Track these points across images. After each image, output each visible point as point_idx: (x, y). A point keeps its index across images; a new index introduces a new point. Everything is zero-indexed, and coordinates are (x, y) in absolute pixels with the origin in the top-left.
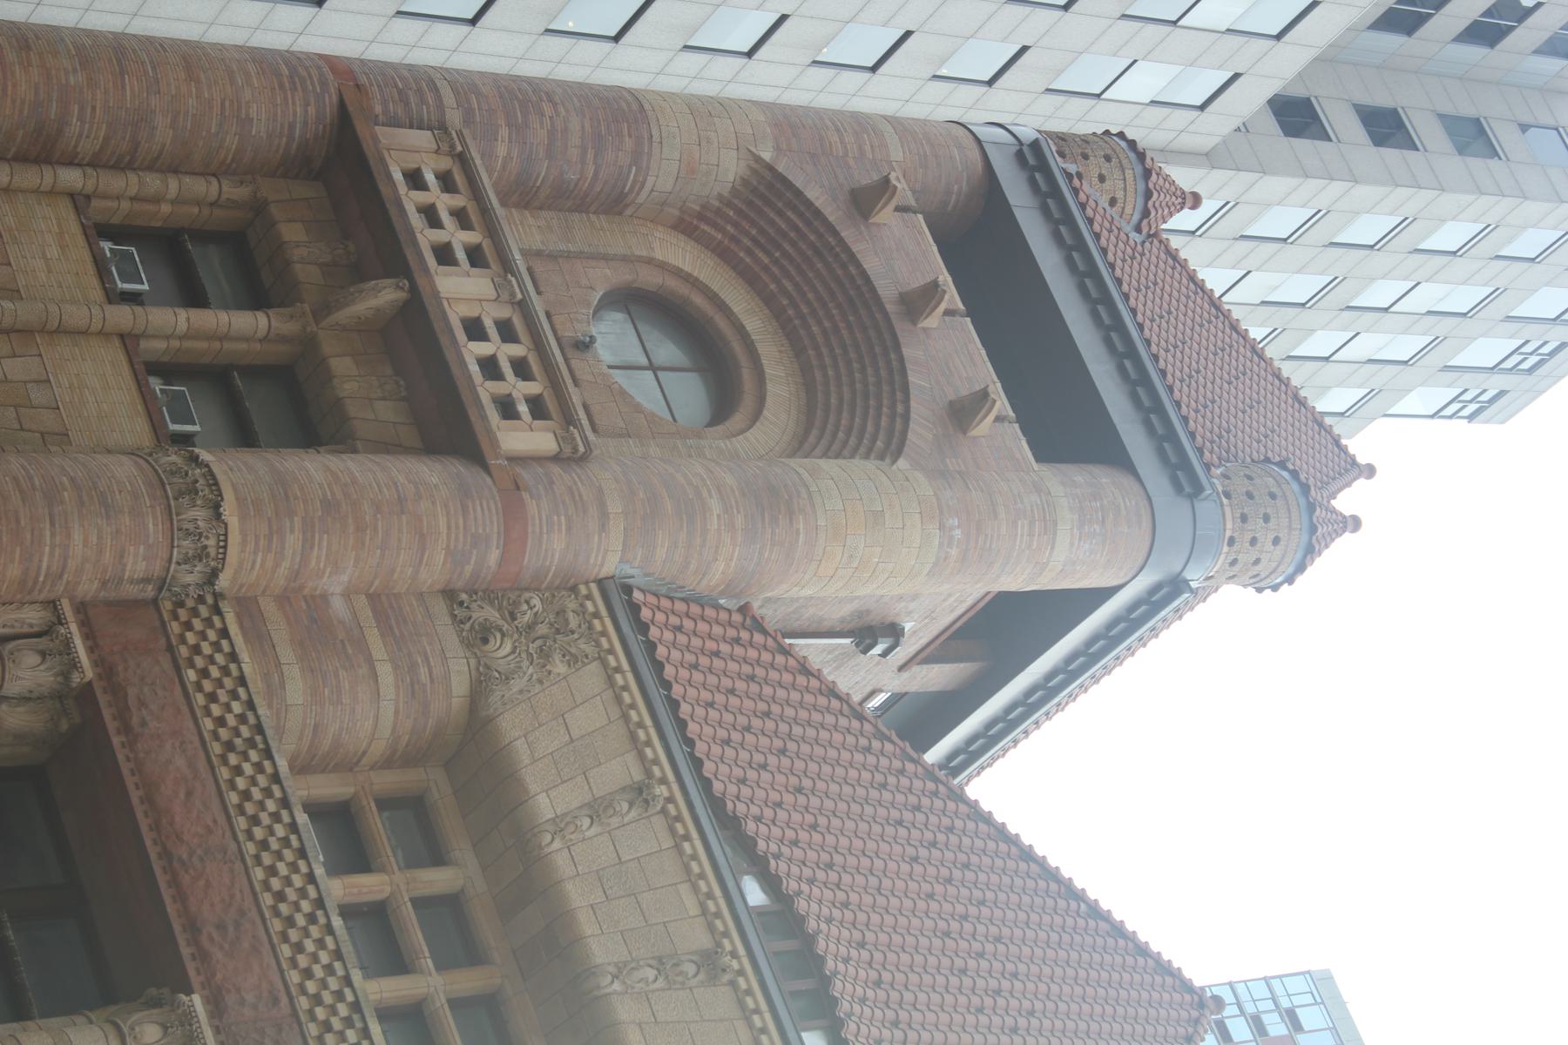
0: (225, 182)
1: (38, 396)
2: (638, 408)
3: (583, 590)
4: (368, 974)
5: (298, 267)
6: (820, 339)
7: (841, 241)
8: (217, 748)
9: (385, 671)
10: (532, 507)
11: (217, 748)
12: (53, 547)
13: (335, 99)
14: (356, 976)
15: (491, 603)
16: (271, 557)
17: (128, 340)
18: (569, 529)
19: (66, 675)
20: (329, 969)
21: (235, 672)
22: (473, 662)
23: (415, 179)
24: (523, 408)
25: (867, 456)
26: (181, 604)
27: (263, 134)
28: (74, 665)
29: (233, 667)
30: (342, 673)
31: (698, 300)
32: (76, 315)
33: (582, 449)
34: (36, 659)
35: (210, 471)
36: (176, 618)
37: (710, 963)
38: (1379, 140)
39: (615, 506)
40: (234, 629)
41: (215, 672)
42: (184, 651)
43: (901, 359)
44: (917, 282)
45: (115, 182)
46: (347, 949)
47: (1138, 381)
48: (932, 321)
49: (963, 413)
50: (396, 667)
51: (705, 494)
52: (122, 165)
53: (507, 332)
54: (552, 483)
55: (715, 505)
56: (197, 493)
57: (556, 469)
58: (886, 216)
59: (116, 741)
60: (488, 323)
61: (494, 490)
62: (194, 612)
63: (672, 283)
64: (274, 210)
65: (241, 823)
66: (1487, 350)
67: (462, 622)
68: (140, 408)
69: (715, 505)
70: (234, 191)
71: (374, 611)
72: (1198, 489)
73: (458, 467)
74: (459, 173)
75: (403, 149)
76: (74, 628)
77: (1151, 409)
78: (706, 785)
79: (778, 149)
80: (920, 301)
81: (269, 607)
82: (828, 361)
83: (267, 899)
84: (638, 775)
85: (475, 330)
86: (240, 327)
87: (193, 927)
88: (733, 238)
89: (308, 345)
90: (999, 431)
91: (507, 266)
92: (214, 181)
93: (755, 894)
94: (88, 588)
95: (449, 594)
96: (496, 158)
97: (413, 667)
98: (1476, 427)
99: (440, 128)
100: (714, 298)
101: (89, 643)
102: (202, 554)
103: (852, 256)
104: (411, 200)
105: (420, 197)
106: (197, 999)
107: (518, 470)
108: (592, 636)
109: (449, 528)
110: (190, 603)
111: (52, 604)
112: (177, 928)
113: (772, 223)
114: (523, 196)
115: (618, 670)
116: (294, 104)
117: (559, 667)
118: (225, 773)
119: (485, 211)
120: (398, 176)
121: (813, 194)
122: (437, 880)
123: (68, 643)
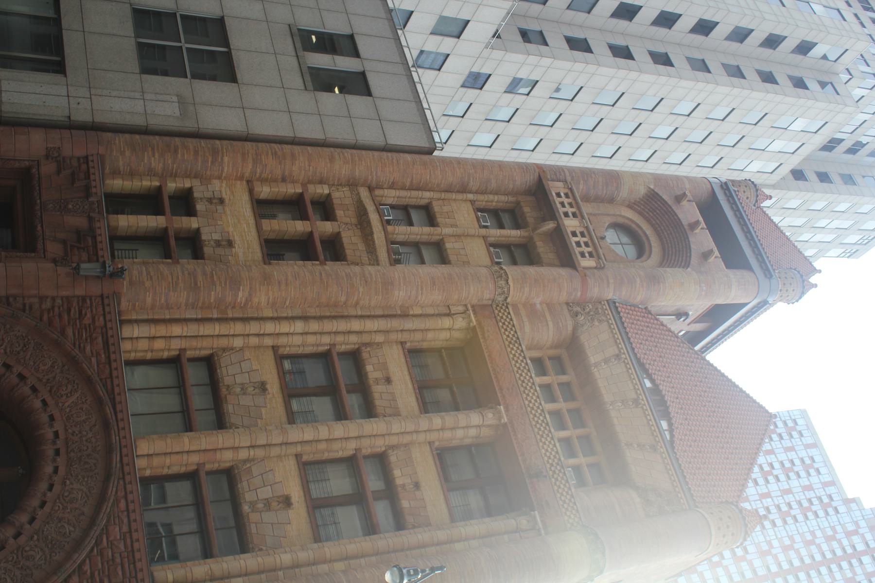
1: (462, 252)
2: (617, 255)
4: (546, 403)
8: (507, 343)
9: (550, 324)
11: (507, 343)
14: (543, 403)
17: (484, 238)
20: (536, 401)
23: (558, 195)
24: (587, 255)
28: (471, 321)
31: (634, 226)
32: (472, 232)
37: (636, 402)
38: (822, 181)
39: (611, 281)
42: (499, 318)
44: (693, 220)
45: (481, 197)
46: (540, 396)
47: (754, 247)
48: (697, 231)
49: (706, 255)
52: (483, 193)
53: (583, 235)
55: (638, 280)
57: (596, 271)
58: (685, 203)
59: (481, 341)
60: (578, 233)
63: (627, 221)
65: (513, 362)
66: (853, 238)
69: (638, 280)
70: (511, 199)
72: (771, 276)
74: (570, 193)
75: (555, 188)
78: (635, 355)
79: (655, 185)
80: (694, 226)
81: (520, 307)
83: (520, 382)
84: (617, 352)
85: (574, 234)
86: (512, 234)
87: (501, 389)
89: (531, 238)
90: (716, 260)
91: (583, 217)
93: (648, 384)
94: (475, 301)
95: (567, 304)
96: (580, 189)
98: (850, 260)
99: (565, 181)
100: (637, 225)
102: (503, 293)
103: (676, 214)
104: (557, 200)
105: (560, 199)
106: (502, 407)
111: (466, 306)
112: (497, 389)
114: (587, 199)
117: (596, 323)
118: (509, 350)
119: (577, 203)
120: (554, 194)
121: (664, 197)
122: (564, 378)
123: (469, 315)
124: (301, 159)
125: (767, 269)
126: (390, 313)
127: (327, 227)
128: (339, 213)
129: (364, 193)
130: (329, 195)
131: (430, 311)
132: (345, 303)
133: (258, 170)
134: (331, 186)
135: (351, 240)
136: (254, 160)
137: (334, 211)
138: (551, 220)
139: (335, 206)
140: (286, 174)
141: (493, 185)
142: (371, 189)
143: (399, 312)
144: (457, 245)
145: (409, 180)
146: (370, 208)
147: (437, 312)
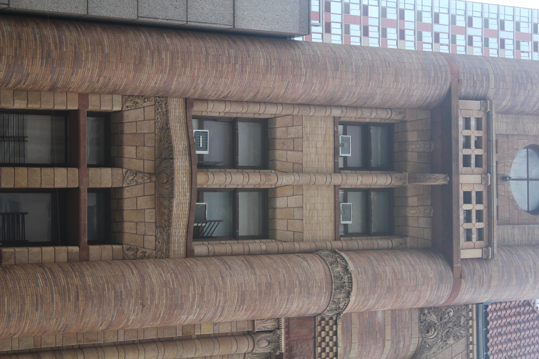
0: (394, 113)
1: (297, 215)
2: (516, 207)
3: (470, 307)
5: (410, 153)
9: (388, 344)
10: (463, 285)
12: (285, 308)
13: (448, 86)
15: (435, 313)
18: (474, 292)
21: (335, 351)
22: (421, 339)
23: (467, 121)
24: (474, 236)
26: (323, 319)
27: (415, 101)
28: (279, 347)
29: (335, 348)
30: (373, 346)
33: (490, 257)
35: (351, 277)
36: (320, 325)
40: (339, 332)
41: (327, 350)
42: (319, 339)
50: (393, 343)
51: (529, 276)
54: (474, 274)
55: (531, 280)
56: (343, 288)
57: (477, 266)
60: (474, 195)
61: (452, 278)
62: (327, 323)
64: (409, 126)
67: (422, 322)
68: (333, 218)
69: (531, 280)
70: (395, 117)
71: (392, 317)
73: (441, 266)
74: (484, 123)
76: (283, 331)
81: (355, 318)
85: (467, 198)
89: (403, 189)
91: (489, 170)
92: (390, 112)
95: (421, 310)
97: (399, 342)
101: (287, 335)
104: (463, 133)
107: (464, 268)
108: (467, 327)
109: (430, 295)
110: (327, 319)
111: (278, 320)
115: (472, 343)
116: (431, 90)
123: (279, 337)
124: (89, 65)
126: (167, 336)
127: (105, 178)
128: (129, 151)
129: (176, 110)
130: (120, 112)
131: (225, 329)
132: (103, 331)
133: (13, 81)
134: (126, 97)
135: (137, 203)
136: (9, 66)
137: (121, 145)
138: (443, 172)
139: (126, 138)
140: (59, 85)
141: (377, 100)
142: (188, 103)
143: (180, 334)
144: (293, 201)
145: (252, 94)
146: (179, 145)
147: (234, 330)
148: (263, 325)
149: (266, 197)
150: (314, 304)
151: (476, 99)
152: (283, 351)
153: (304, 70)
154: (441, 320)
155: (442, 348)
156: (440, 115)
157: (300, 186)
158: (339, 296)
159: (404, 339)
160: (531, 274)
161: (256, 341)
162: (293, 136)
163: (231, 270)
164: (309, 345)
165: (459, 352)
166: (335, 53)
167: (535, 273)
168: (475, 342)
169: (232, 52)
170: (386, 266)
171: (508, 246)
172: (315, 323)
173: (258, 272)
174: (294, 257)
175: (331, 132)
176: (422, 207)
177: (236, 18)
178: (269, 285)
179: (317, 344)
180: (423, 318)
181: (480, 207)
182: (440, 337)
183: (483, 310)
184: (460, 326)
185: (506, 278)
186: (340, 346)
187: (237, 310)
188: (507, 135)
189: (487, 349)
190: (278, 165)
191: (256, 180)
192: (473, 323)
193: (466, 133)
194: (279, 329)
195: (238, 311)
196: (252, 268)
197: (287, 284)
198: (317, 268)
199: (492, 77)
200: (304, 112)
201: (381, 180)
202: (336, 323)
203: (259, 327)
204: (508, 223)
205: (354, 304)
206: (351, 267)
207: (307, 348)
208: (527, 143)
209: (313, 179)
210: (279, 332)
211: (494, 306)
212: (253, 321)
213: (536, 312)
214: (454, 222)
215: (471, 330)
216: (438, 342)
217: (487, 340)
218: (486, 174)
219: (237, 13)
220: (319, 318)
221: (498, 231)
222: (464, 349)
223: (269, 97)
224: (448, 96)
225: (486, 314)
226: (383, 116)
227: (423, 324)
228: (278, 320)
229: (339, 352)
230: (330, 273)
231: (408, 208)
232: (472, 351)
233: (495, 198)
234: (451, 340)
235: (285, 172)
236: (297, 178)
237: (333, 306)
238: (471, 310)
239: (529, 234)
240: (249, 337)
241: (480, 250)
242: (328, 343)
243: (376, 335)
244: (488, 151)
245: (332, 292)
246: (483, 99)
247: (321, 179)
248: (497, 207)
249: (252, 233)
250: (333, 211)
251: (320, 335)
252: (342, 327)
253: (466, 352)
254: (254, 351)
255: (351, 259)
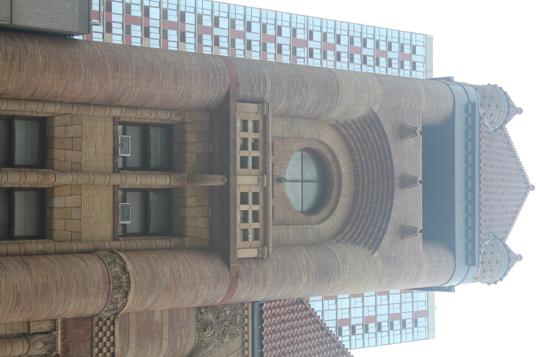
0: (173, 114)
1: (75, 215)
2: (291, 208)
3: (246, 305)
5: (188, 154)
6: (366, 184)
7: (389, 149)
9: (165, 343)
10: (240, 284)
13: (226, 89)
16: (140, 306)
18: (250, 291)
19: (51, 351)
22: (198, 338)
23: (245, 123)
24: (251, 236)
25: (364, 246)
26: (101, 319)
27: (194, 102)
28: (55, 348)
29: (112, 348)
30: (150, 345)
31: (329, 156)
33: (266, 256)
34: (42, 345)
35: (129, 277)
36: (97, 325)
40: (117, 332)
41: (105, 350)
42: (96, 340)
43: (392, 205)
49: (405, 232)
50: (170, 342)
51: (303, 275)
54: (250, 273)
55: (304, 279)
61: (229, 278)
62: (105, 324)
64: (187, 126)
67: (199, 321)
68: (111, 218)
69: (304, 279)
70: (175, 118)
73: (218, 265)
76: (59, 332)
77: (470, 241)
80: (407, 182)
81: (132, 318)
82: (365, 194)
85: (244, 199)
88: (351, 135)
89: (181, 189)
91: (265, 172)
92: (169, 113)
95: (199, 309)
101: (63, 336)
103: (391, 156)
108: (243, 325)
109: (207, 294)
110: (104, 319)
111: (54, 321)
113: (367, 134)
115: (247, 341)
116: (210, 92)
123: (55, 338)
125: (473, 253)
138: (221, 173)
144: (71, 201)
145: (29, 92)
147: (9, 332)
148: (39, 326)
149: (43, 197)
150: (92, 304)
151: (253, 102)
152: (59, 353)
153: (83, 69)
154: (218, 319)
155: (218, 346)
156: (219, 116)
157: (79, 186)
158: (117, 296)
159: (182, 338)
160: (304, 274)
161: (31, 343)
162: (71, 135)
163: (6, 270)
164: (85, 346)
165: (234, 350)
166: (115, 53)
167: (308, 272)
168: (250, 340)
169: (10, 48)
170: (164, 265)
171: (283, 246)
172: (92, 323)
173: (34, 272)
174: (72, 258)
175: (111, 132)
176: (201, 208)
177: (13, 14)
178: (46, 286)
179: (94, 345)
180: (200, 316)
181: (256, 208)
182: (216, 335)
183: (258, 308)
184: (236, 324)
185: (280, 276)
186: (118, 346)
187: (12, 311)
188: (283, 138)
189: (262, 346)
190: (57, 164)
191: (33, 179)
192: (248, 321)
193: (244, 135)
194: (55, 330)
195: (13, 312)
196: (29, 268)
197: (64, 285)
198: (95, 268)
199: (269, 81)
200: (83, 111)
201: (161, 181)
202: (113, 323)
203: (34, 328)
204: (283, 223)
205: (132, 304)
206: (129, 267)
207: (84, 349)
208: (302, 146)
209: (92, 178)
210: (55, 333)
211: (269, 304)
212: (29, 323)
213: (308, 309)
214: (232, 223)
215: (246, 327)
216: (215, 340)
217: (262, 338)
218: (262, 175)
219: (15, 9)
220: (96, 319)
221: (273, 231)
222: (240, 346)
223: (47, 95)
224: (227, 98)
225: (261, 312)
226: (162, 117)
227: (200, 323)
228: (54, 321)
229: (116, 353)
230: (108, 273)
231: (186, 209)
232: (247, 349)
233: (271, 199)
234: (227, 338)
235: (63, 172)
236: (75, 177)
237: (111, 307)
238: (247, 309)
239: (303, 234)
240: (24, 339)
241: (257, 250)
242: (105, 343)
243: (154, 334)
244: (265, 153)
245: (110, 292)
246: (260, 102)
247: (100, 180)
248: (273, 208)
249: (28, 233)
250: (111, 211)
251: (97, 336)
252: (120, 327)
253: (241, 350)
254: (29, 353)
255: (129, 259)
